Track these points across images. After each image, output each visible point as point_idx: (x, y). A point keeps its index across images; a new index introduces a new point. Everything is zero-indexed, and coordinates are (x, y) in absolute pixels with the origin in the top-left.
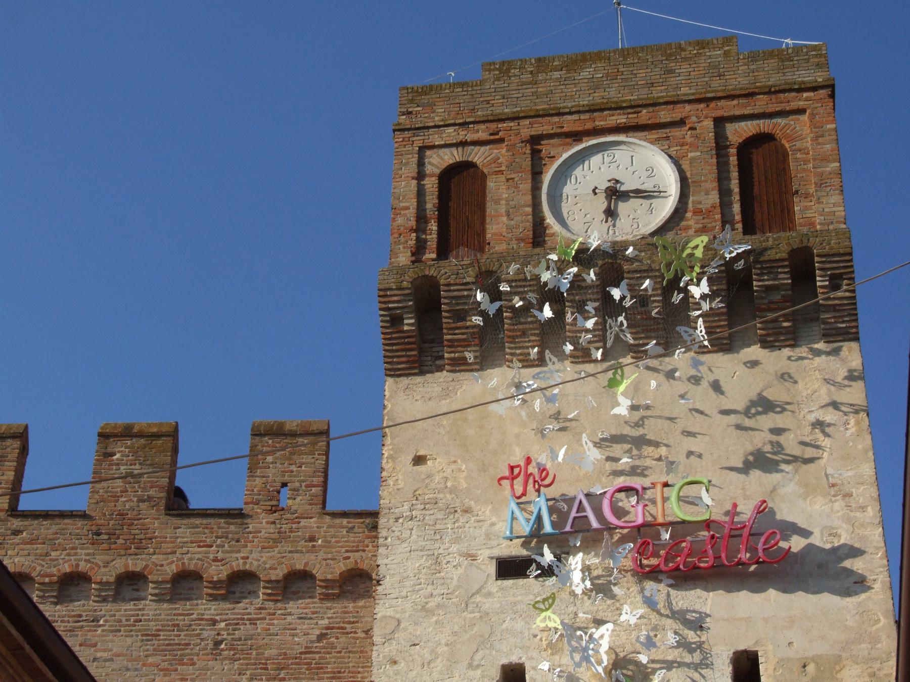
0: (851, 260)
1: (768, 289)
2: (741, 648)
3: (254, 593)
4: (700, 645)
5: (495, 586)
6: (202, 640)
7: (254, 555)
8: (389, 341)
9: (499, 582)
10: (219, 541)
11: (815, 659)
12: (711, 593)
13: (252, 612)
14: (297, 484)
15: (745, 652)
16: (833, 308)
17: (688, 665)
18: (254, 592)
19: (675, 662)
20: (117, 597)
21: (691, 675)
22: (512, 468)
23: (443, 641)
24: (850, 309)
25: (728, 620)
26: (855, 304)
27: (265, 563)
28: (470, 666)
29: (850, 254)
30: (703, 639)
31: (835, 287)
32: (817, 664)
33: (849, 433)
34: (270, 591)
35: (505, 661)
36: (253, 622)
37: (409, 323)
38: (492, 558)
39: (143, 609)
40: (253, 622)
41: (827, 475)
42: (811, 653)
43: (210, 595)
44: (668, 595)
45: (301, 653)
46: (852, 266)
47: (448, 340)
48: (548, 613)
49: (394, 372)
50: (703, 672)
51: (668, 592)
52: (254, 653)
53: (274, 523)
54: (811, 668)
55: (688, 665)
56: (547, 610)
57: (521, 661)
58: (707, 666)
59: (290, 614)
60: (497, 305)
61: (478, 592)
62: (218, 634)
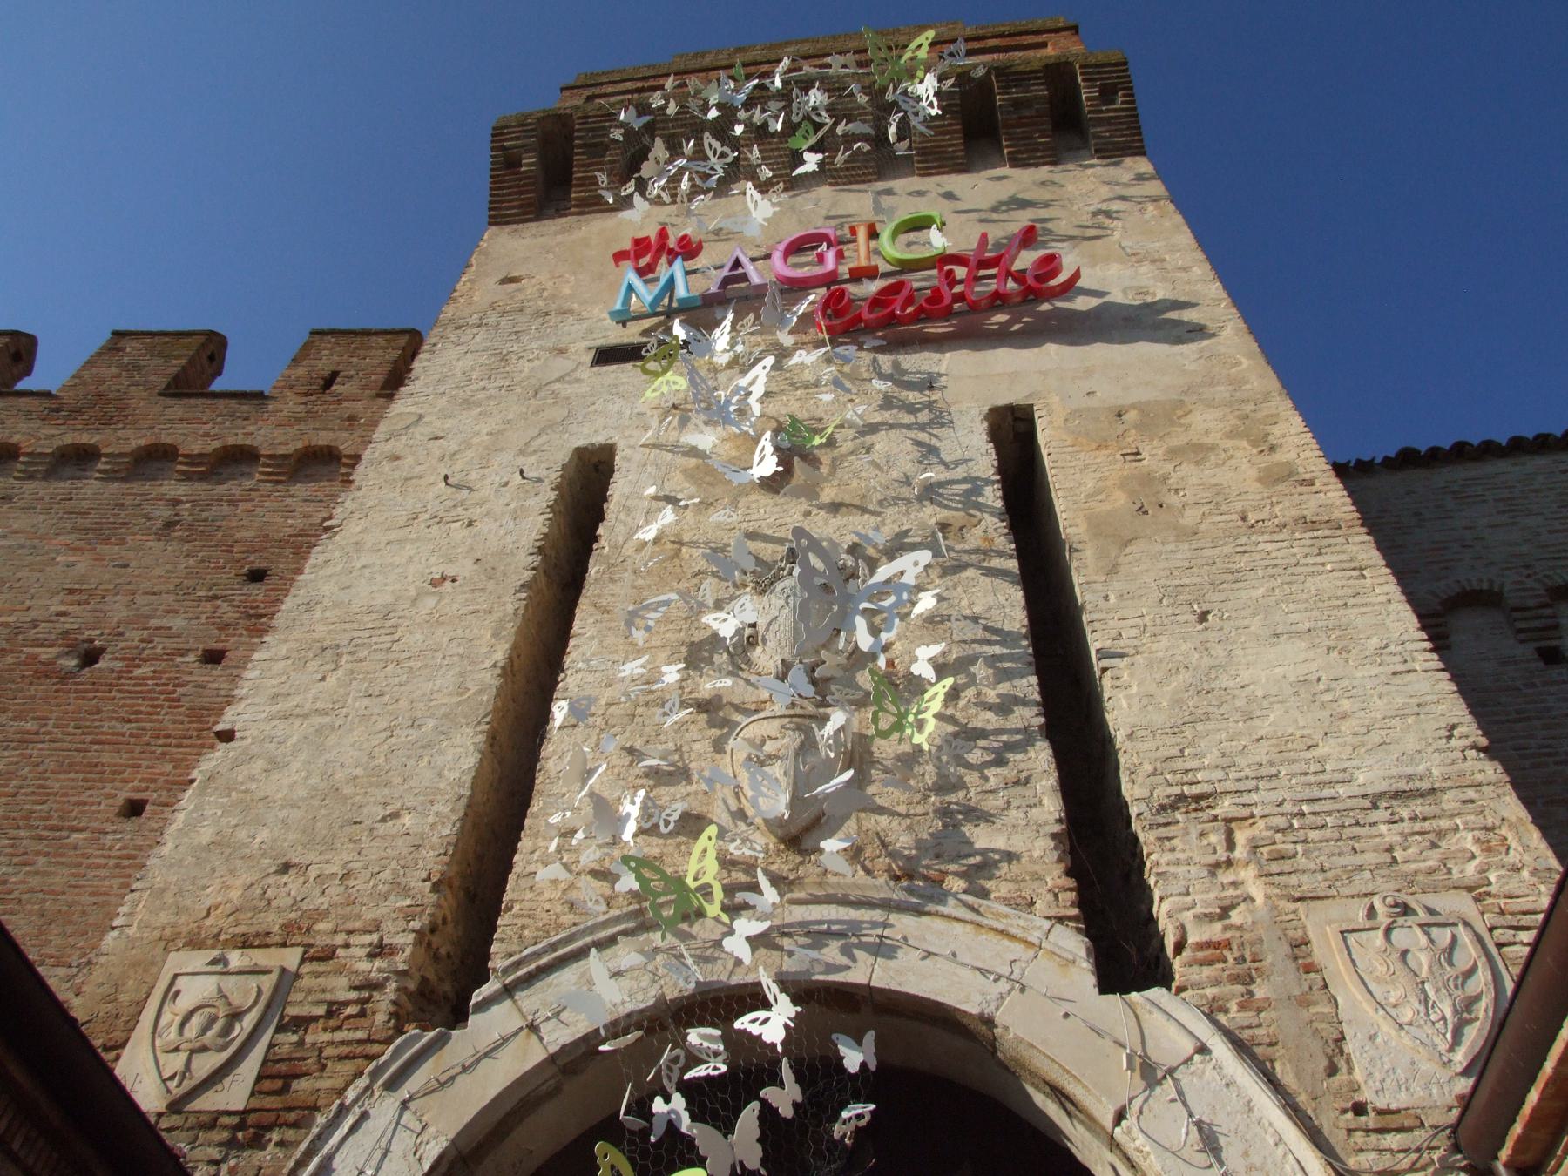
0: (1127, 70)
1: (1017, 104)
2: (1002, 401)
3: (250, 476)
4: (929, 406)
5: (588, 374)
6: (149, 519)
7: (262, 432)
8: (497, 183)
9: (596, 369)
10: (219, 419)
11: (1133, 406)
12: (948, 355)
13: (238, 492)
14: (352, 372)
15: (1011, 409)
16: (1108, 121)
17: (908, 427)
18: (249, 474)
19: (886, 424)
20: (50, 474)
21: (913, 436)
22: (637, 242)
23: (485, 431)
24: (1132, 117)
25: (977, 376)
26: (1137, 116)
27: (274, 439)
28: (522, 452)
29: (1125, 63)
30: (933, 398)
31: (1107, 94)
32: (1141, 411)
33: (1147, 216)
34: (270, 470)
35: (581, 443)
36: (233, 503)
37: (529, 162)
38: (590, 349)
39: (81, 488)
40: (233, 503)
41: (1123, 248)
42: (1129, 401)
43: (183, 473)
44: (875, 360)
45: (290, 536)
46: (1127, 70)
47: (579, 178)
48: (669, 376)
49: (499, 217)
50: (935, 432)
51: (875, 360)
52: (220, 534)
53: (305, 404)
54: (1131, 416)
55: (908, 427)
56: (665, 371)
57: (610, 442)
58: (942, 425)
59: (292, 496)
60: (646, 119)
61: (558, 380)
62: (176, 515)
